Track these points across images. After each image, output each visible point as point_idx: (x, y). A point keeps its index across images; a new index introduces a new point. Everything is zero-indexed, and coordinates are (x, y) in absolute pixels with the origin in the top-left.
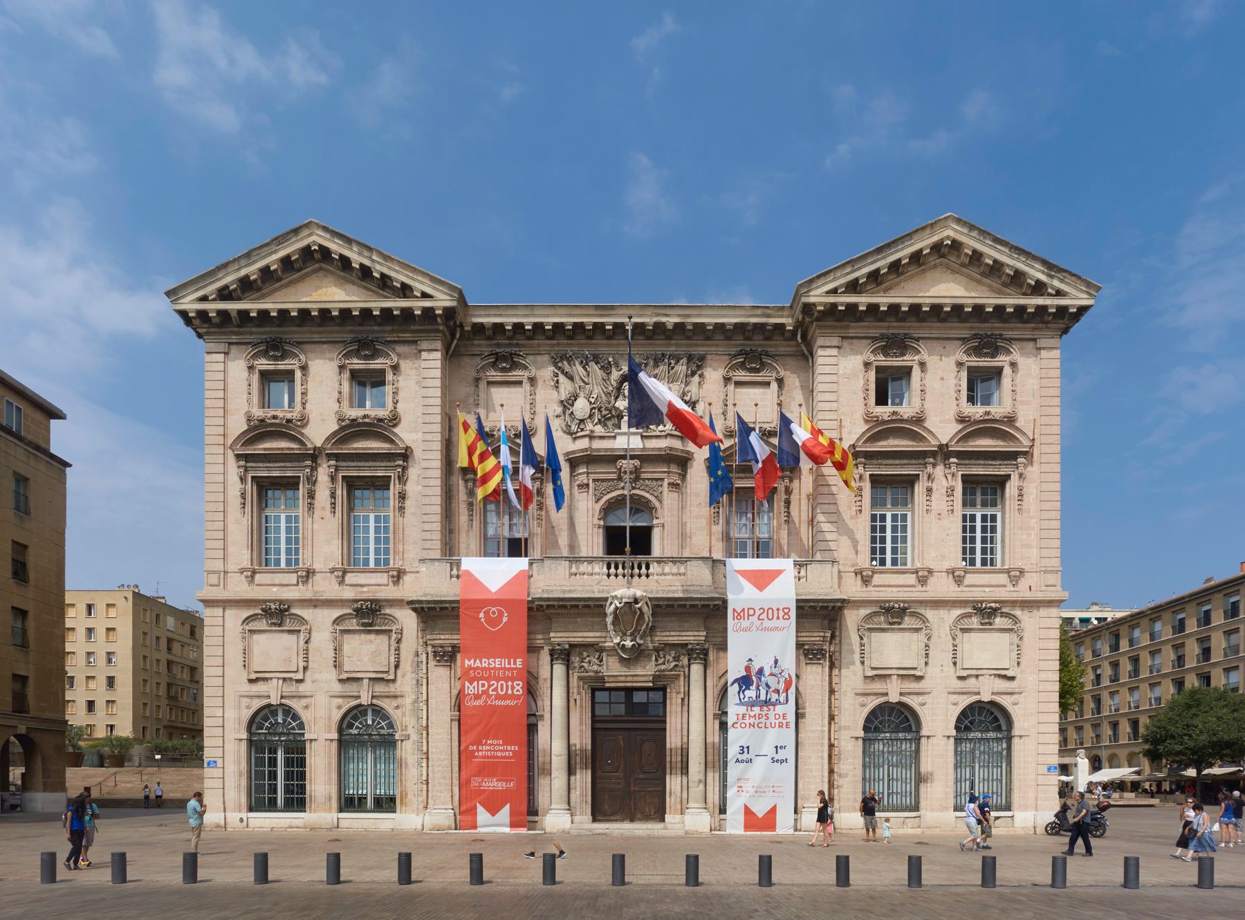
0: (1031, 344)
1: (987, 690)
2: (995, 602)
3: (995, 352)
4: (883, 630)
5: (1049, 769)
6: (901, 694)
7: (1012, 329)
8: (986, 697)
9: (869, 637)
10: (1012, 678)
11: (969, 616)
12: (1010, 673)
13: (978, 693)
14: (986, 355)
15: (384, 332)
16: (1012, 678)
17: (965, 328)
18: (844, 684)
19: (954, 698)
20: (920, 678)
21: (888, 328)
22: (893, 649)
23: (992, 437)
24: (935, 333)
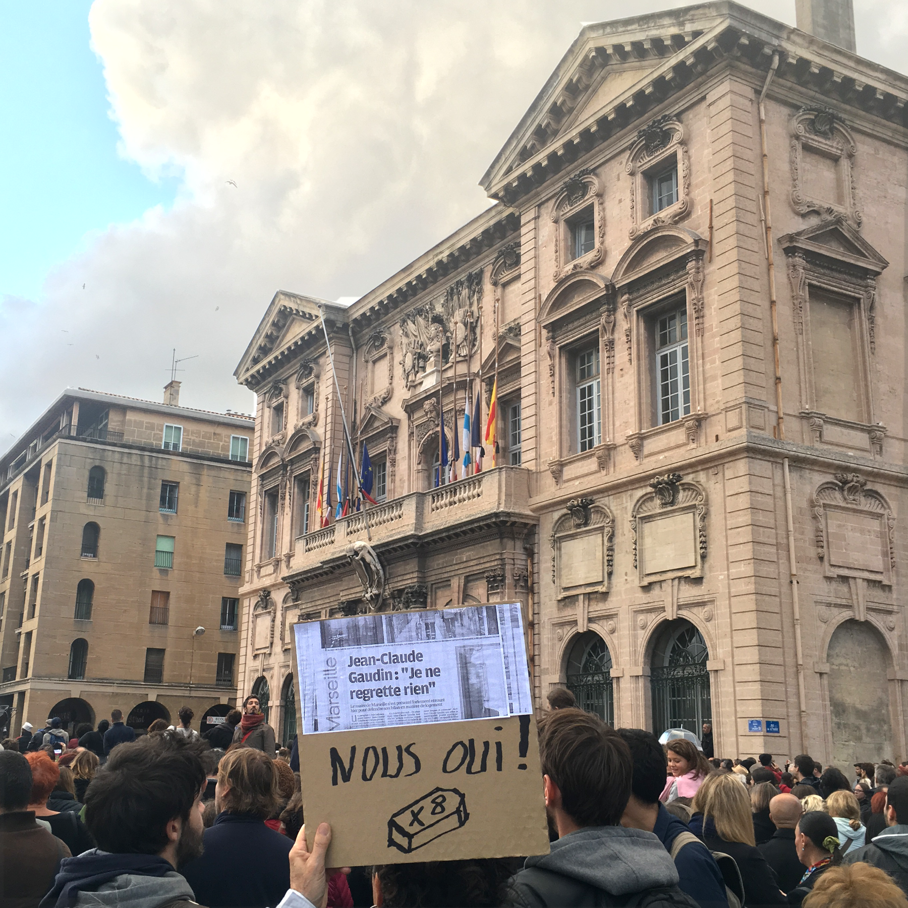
0: (704, 105)
1: (670, 602)
2: (669, 471)
3: (666, 137)
4: (572, 537)
5: (751, 725)
6: (590, 620)
7: (676, 101)
8: (670, 615)
9: (560, 549)
10: (698, 581)
11: (651, 499)
12: (696, 573)
13: (663, 609)
14: (657, 148)
15: (312, 352)
16: (698, 581)
17: (631, 131)
18: (543, 613)
19: (641, 618)
20: (605, 595)
21: (568, 173)
22: (581, 559)
23: (665, 248)
24: (608, 154)
